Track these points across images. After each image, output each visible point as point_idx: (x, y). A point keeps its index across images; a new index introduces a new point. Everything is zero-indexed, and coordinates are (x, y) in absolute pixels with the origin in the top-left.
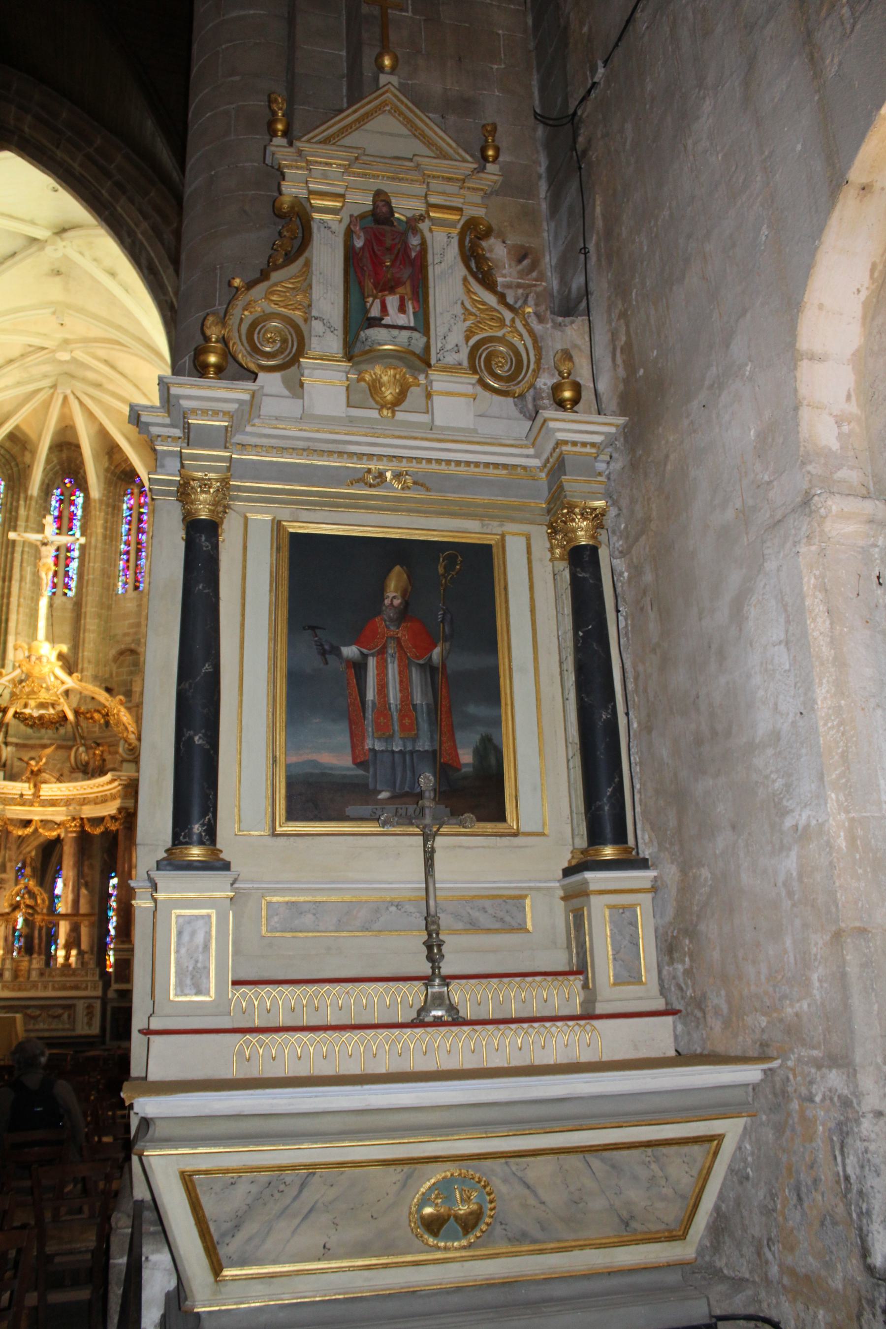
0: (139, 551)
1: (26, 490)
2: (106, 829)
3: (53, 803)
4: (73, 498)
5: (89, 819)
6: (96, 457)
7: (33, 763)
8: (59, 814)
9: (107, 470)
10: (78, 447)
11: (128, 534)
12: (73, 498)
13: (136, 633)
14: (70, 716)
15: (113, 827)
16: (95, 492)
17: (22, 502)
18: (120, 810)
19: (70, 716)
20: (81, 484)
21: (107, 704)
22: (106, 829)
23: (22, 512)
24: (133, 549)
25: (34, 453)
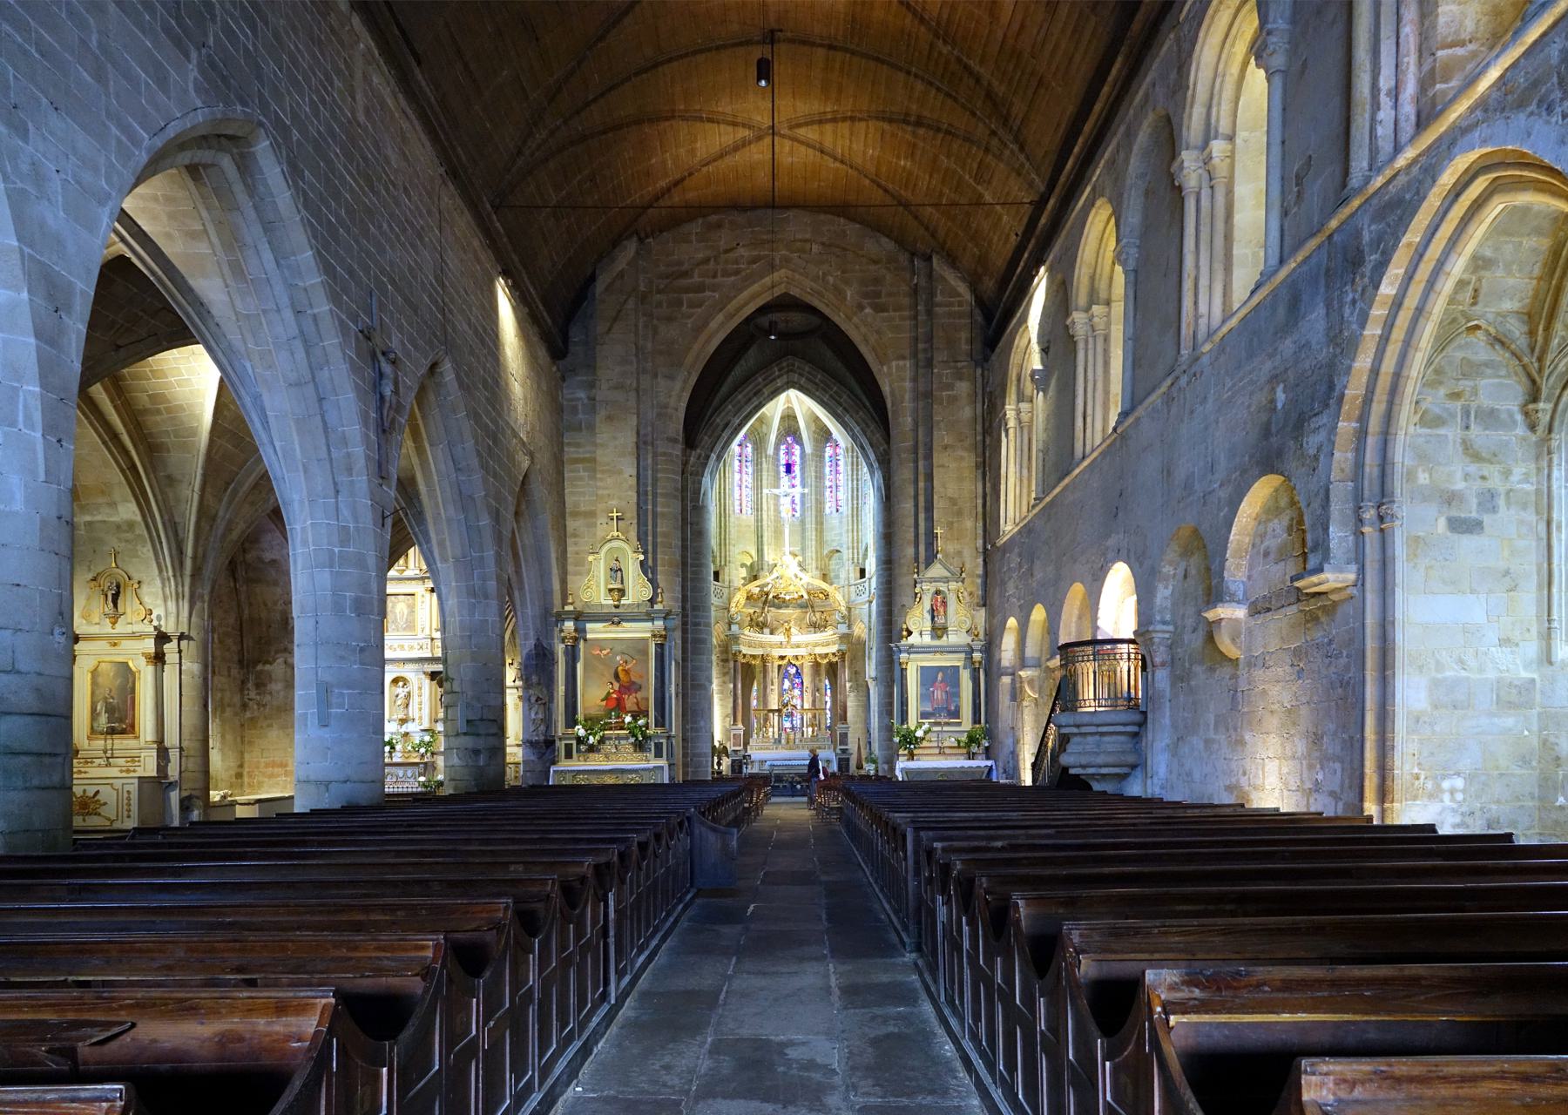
6: (808, 427)
8: (801, 652)
10: (795, 417)
16: (808, 449)
19: (806, 597)
20: (798, 440)
24: (833, 484)
25: (769, 426)
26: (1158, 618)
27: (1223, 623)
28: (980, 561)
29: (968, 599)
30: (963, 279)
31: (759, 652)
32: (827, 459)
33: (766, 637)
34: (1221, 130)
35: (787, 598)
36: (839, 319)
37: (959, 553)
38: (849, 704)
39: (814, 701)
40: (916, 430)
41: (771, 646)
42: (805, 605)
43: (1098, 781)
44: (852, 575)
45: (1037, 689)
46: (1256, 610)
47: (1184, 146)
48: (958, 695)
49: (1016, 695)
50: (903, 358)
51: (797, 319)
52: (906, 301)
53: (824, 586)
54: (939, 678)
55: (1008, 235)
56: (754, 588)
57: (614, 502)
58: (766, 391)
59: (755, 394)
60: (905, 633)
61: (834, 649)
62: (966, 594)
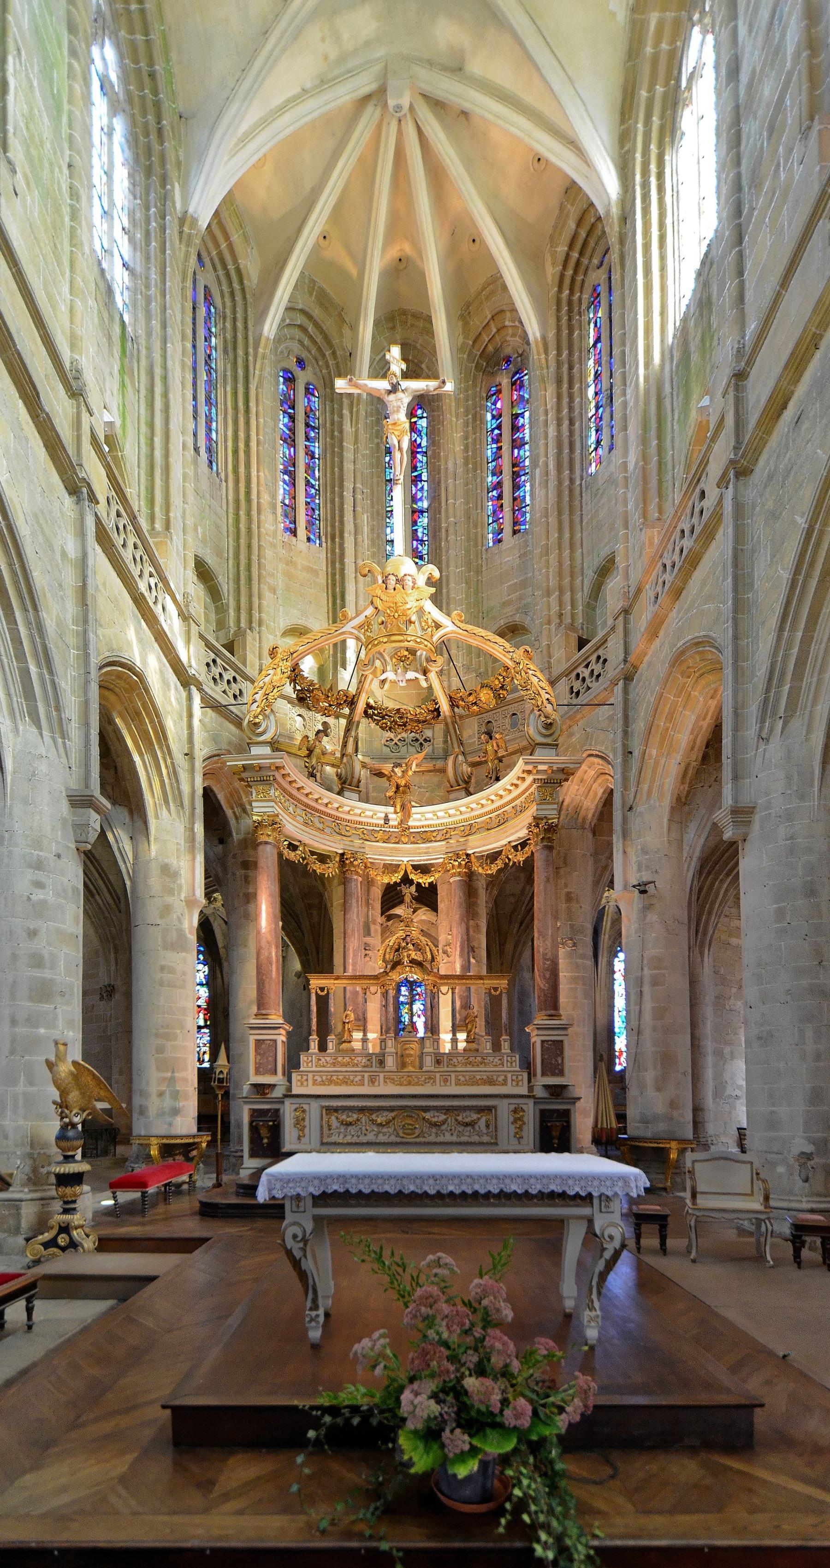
14: (445, 706)
19: (445, 706)
23: (347, 427)
31: (332, 845)
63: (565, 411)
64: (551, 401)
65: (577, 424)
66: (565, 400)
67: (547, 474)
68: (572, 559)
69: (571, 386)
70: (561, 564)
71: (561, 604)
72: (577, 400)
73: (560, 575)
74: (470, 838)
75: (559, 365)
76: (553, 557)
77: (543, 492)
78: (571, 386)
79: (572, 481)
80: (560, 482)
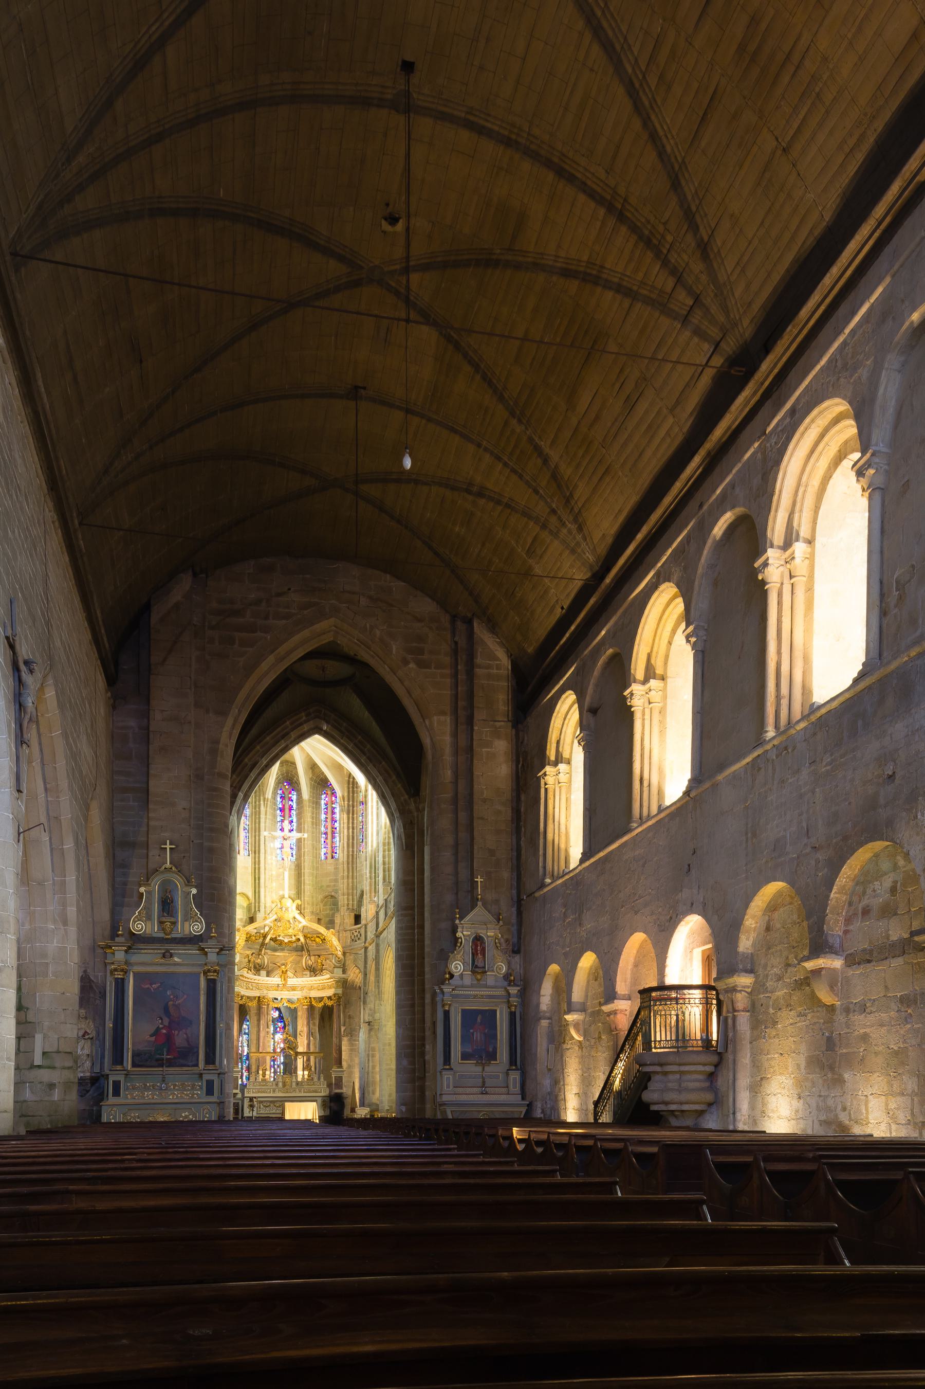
0: (333, 833)
1: (264, 794)
2: (325, 1004)
3: (293, 989)
4: (290, 796)
5: (314, 998)
6: (306, 773)
7: (283, 967)
8: (296, 995)
9: (311, 779)
11: (326, 821)
12: (290, 796)
13: (334, 886)
15: (330, 1003)
17: (262, 802)
18: (335, 995)
19: (302, 939)
21: (325, 934)
22: (325, 1004)
26: (741, 967)
27: (823, 972)
28: (514, 910)
29: (504, 945)
30: (502, 644)
31: (256, 993)
32: (323, 806)
33: (262, 979)
34: (802, 534)
35: (286, 941)
36: (384, 671)
37: (497, 902)
38: (343, 1048)
39: (309, 1045)
40: (456, 783)
41: (268, 989)
42: (300, 949)
43: (676, 1117)
44: (347, 921)
45: (581, 1032)
46: (851, 961)
47: (768, 545)
48: (495, 1036)
49: (558, 1037)
50: (443, 713)
51: (335, 669)
52: (447, 660)
53: (322, 930)
54: (479, 1020)
55: (553, 608)
56: (251, 928)
57: (167, 834)
58: (293, 735)
59: (283, 737)
60: (447, 976)
61: (330, 992)
62: (502, 940)
63: (351, 825)
64: (346, 821)
65: (355, 831)
66: (351, 821)
67: (344, 847)
68: (353, 882)
69: (353, 814)
70: (348, 884)
71: (348, 900)
72: (355, 821)
73: (348, 889)
74: (311, 991)
75: (348, 805)
76: (346, 881)
77: (342, 854)
78: (353, 814)
79: (353, 851)
80: (348, 852)
